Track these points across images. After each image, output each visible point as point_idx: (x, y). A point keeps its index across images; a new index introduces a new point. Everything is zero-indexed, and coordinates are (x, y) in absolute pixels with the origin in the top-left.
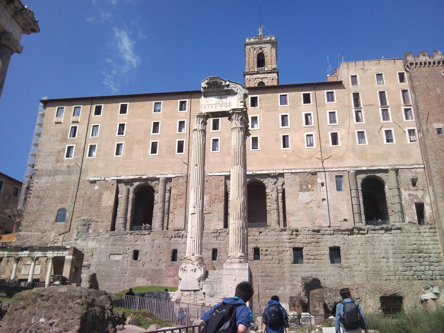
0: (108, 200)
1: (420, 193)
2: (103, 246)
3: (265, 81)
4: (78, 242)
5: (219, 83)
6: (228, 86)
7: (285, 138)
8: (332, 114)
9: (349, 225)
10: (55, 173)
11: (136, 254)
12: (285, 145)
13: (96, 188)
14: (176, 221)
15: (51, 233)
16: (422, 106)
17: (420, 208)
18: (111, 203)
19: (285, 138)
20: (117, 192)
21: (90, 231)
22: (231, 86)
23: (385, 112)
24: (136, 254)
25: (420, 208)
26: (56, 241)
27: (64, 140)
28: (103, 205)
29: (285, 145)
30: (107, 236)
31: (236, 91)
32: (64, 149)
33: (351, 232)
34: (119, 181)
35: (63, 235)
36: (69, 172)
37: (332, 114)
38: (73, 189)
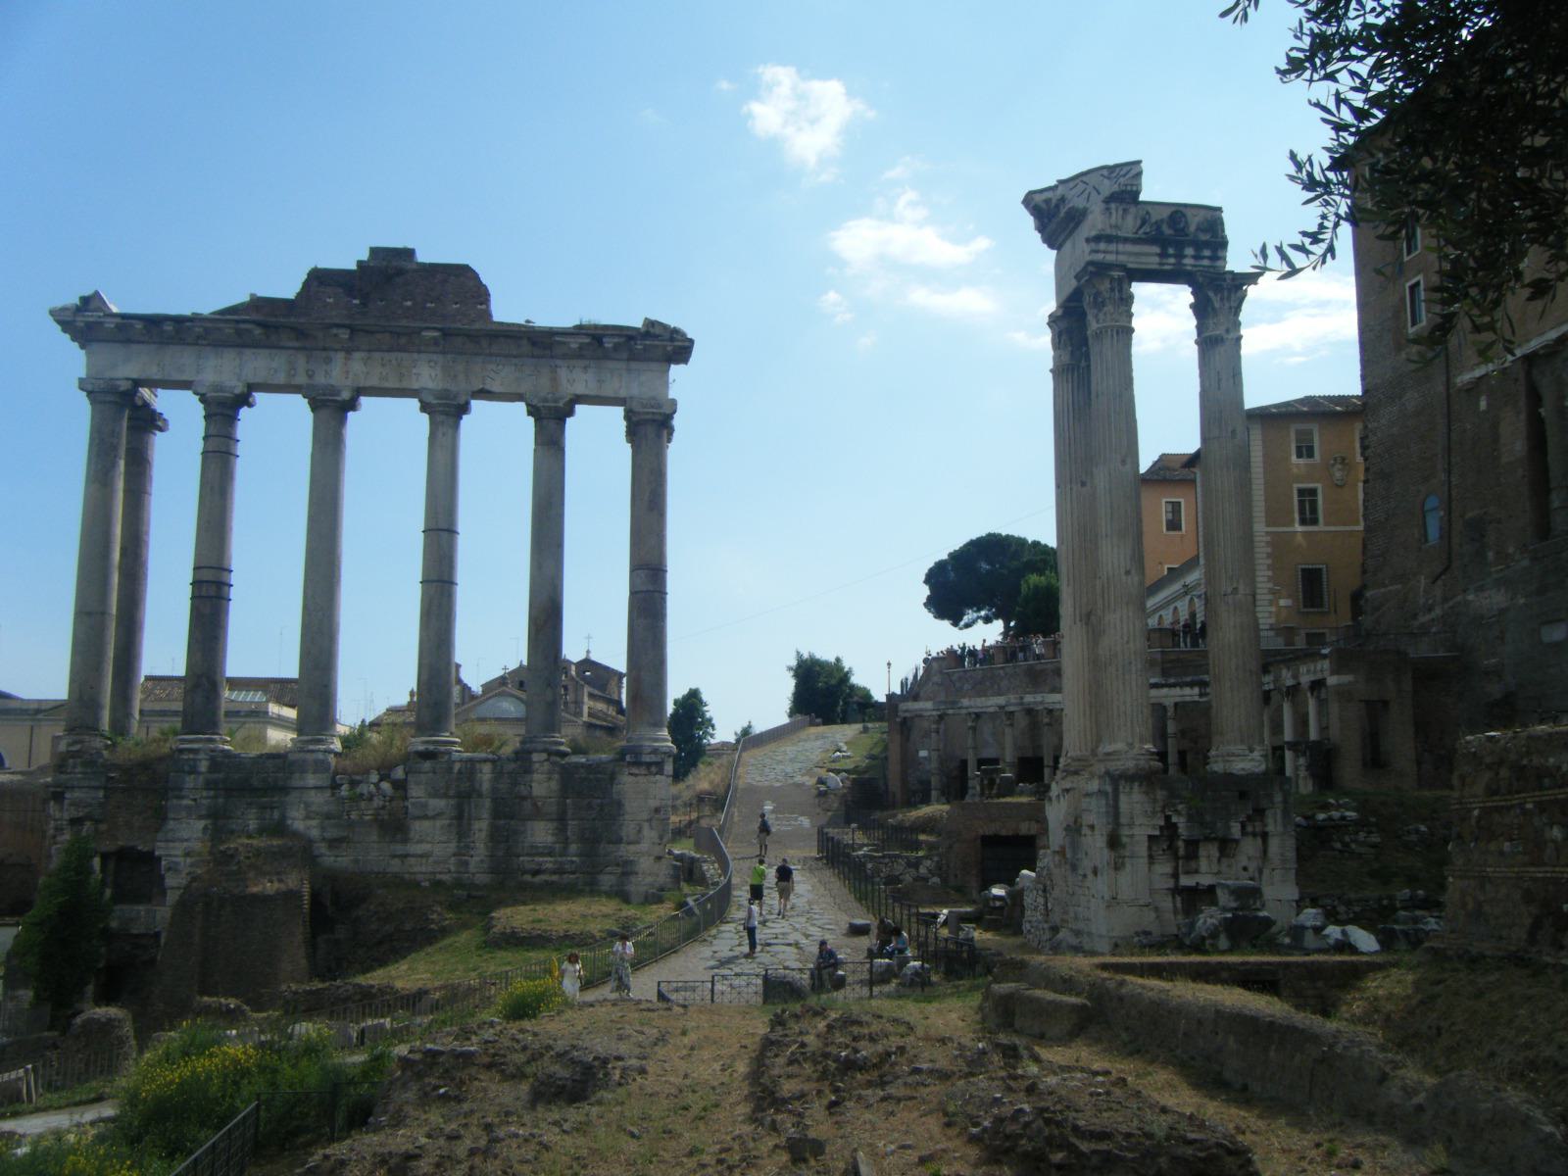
2: (1522, 601)
4: (1471, 597)
5: (1044, 206)
6: (1063, 199)
13: (1483, 404)
15: (1419, 581)
20: (1535, 398)
21: (1491, 555)
22: (1069, 195)
26: (1430, 602)
28: (1504, 460)
30: (1525, 563)
31: (1081, 206)
32: (1403, 299)
34: (1530, 359)
35: (1439, 582)
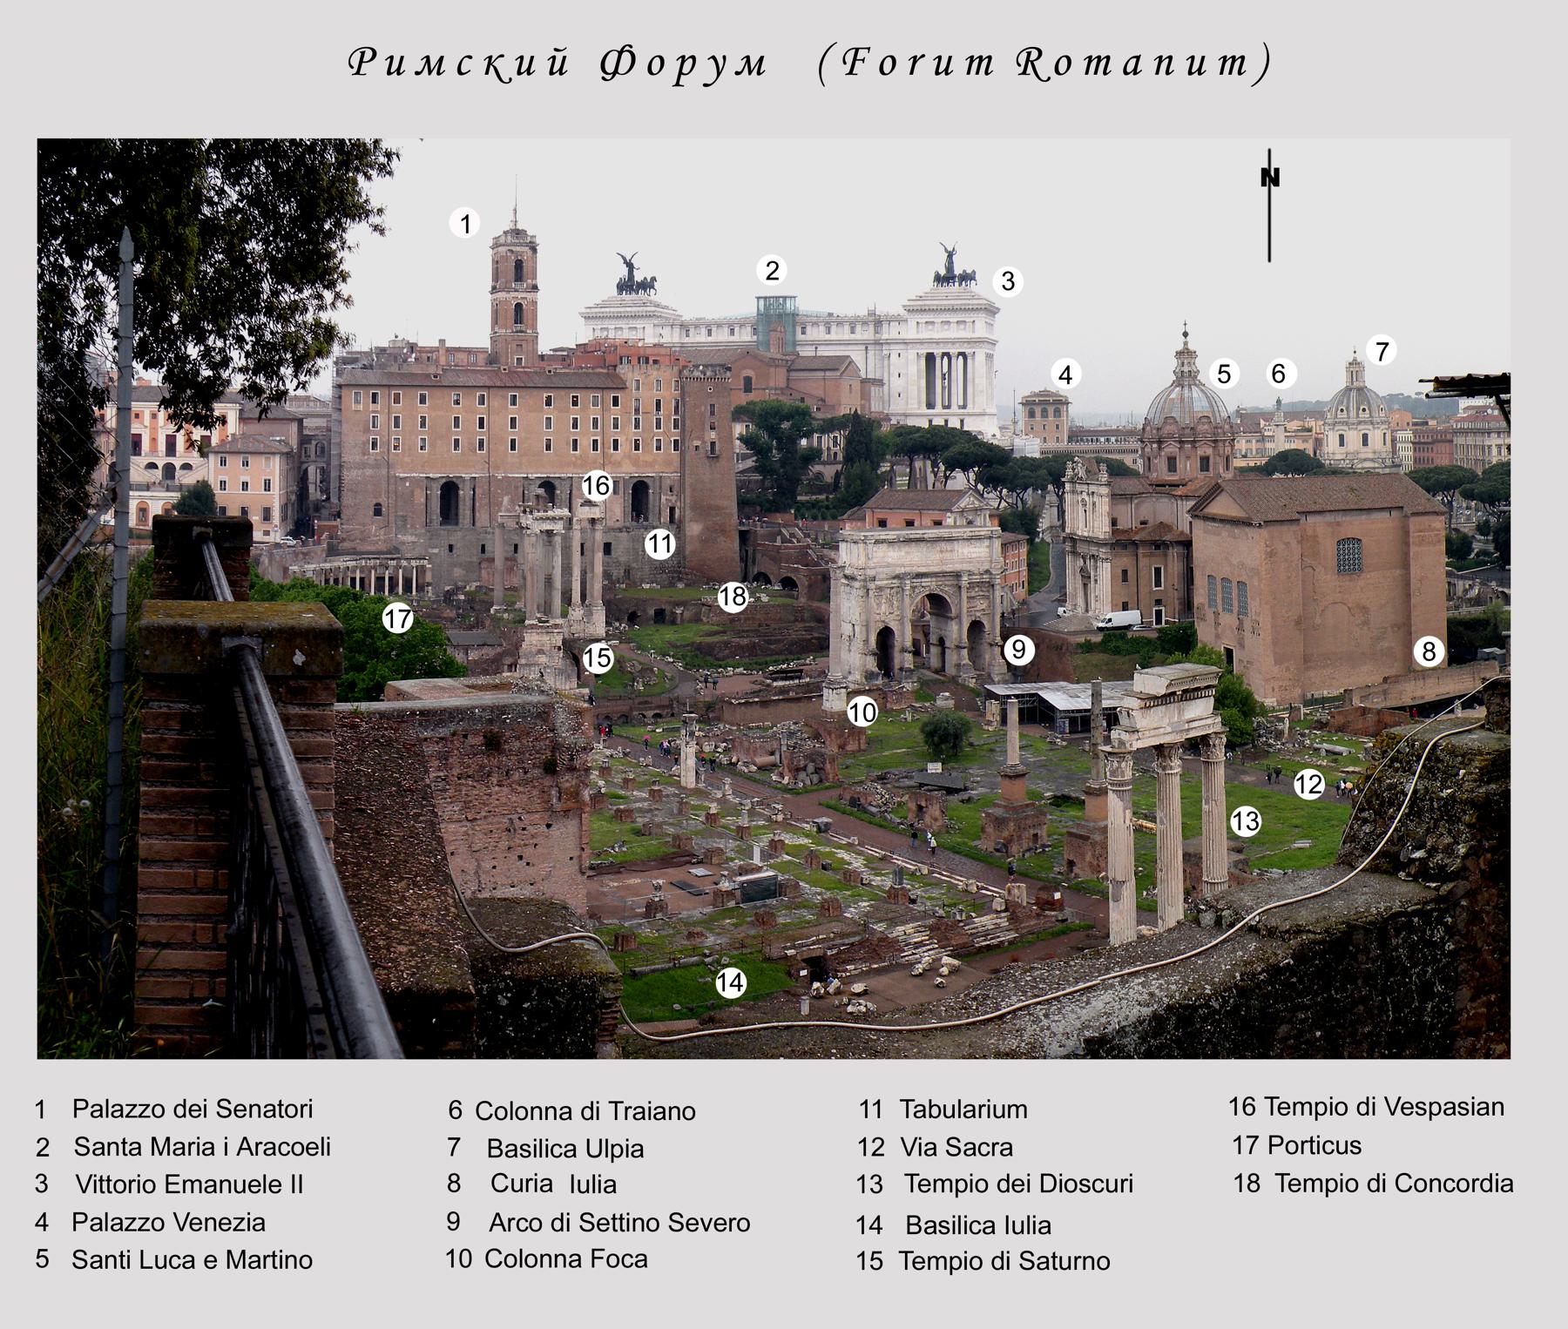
0: (420, 498)
1: (674, 498)
3: (524, 303)
7: (575, 441)
8: (616, 419)
9: (618, 525)
10: (362, 466)
11: (451, 548)
12: (575, 449)
14: (483, 518)
16: (688, 423)
17: (672, 509)
18: (423, 500)
19: (575, 441)
23: (659, 421)
24: (451, 548)
25: (672, 509)
27: (367, 430)
29: (575, 449)
33: (620, 530)
36: (377, 466)
37: (616, 419)
38: (384, 485)
